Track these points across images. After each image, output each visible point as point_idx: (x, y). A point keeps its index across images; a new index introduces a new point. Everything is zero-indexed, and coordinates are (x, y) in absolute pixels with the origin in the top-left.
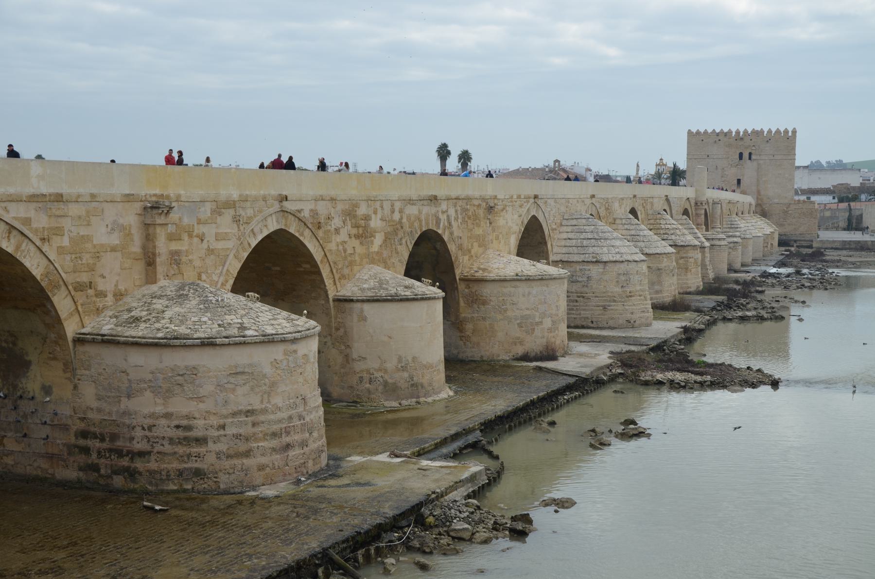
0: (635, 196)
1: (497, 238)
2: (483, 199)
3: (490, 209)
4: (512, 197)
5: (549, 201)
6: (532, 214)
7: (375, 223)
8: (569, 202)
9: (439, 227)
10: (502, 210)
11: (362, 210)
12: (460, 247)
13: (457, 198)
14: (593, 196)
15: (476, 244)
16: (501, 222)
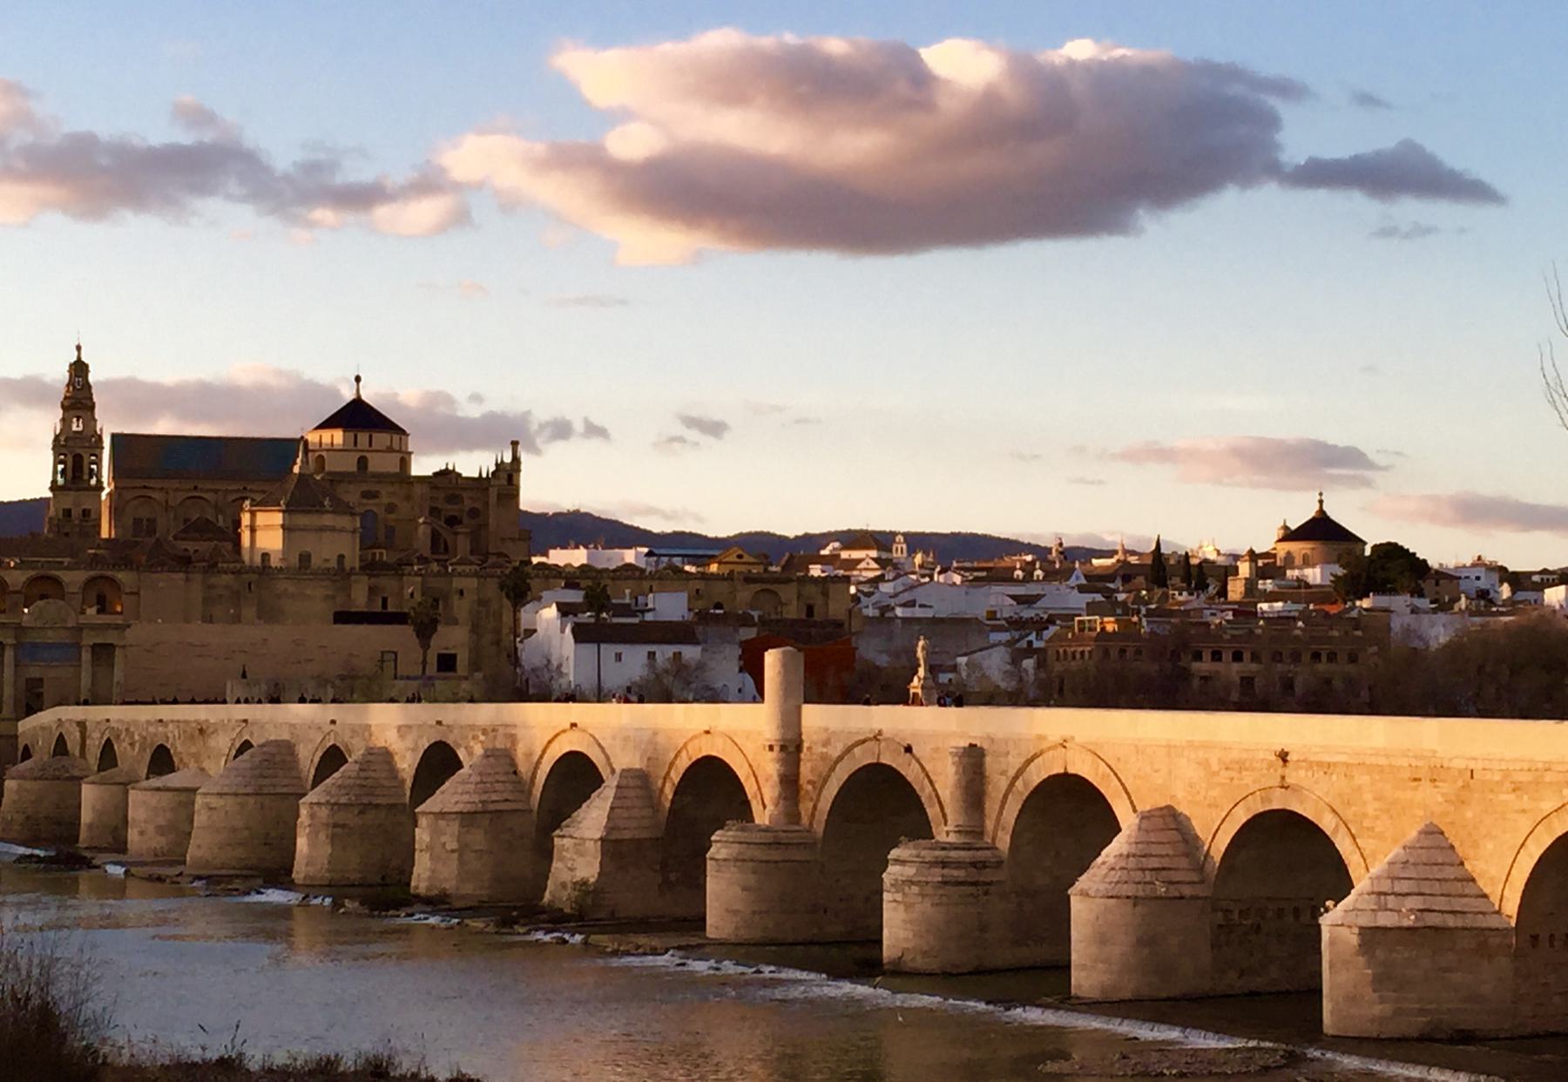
0: (439, 723)
1: (209, 757)
2: (196, 721)
3: (201, 731)
4: (223, 721)
5: (267, 726)
6: (245, 738)
7: (137, 737)
8: (295, 728)
9: (168, 741)
10: (213, 733)
11: (132, 729)
12: (181, 760)
13: (178, 721)
14: (333, 722)
15: (192, 760)
16: (212, 743)
